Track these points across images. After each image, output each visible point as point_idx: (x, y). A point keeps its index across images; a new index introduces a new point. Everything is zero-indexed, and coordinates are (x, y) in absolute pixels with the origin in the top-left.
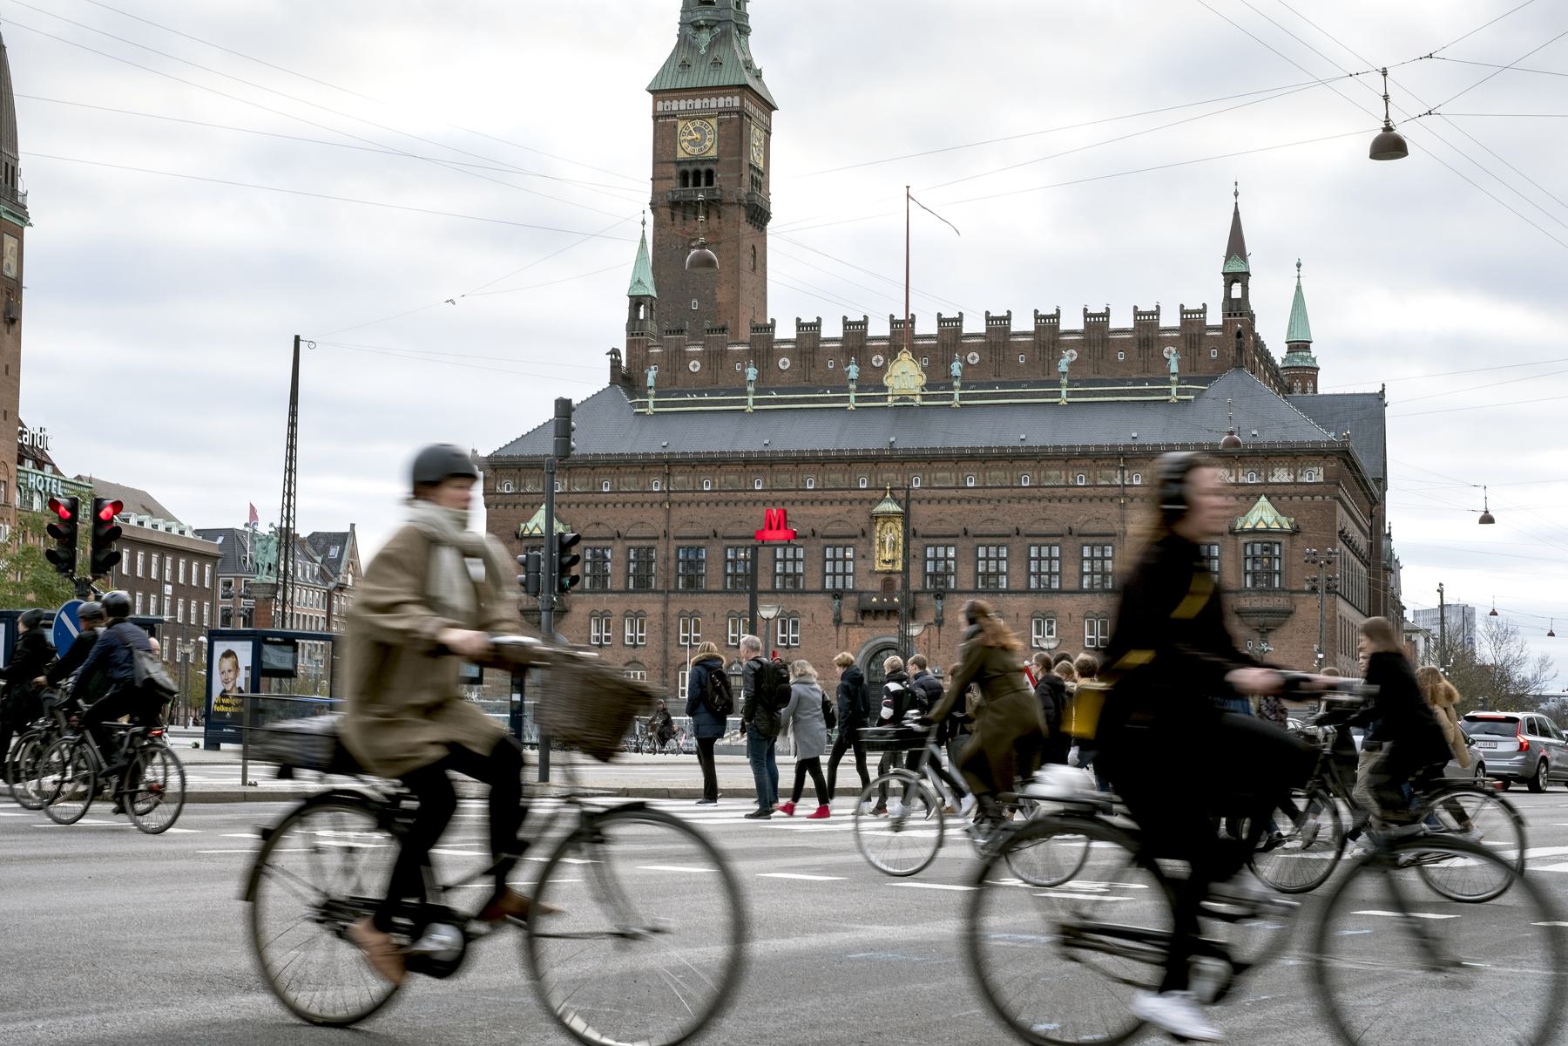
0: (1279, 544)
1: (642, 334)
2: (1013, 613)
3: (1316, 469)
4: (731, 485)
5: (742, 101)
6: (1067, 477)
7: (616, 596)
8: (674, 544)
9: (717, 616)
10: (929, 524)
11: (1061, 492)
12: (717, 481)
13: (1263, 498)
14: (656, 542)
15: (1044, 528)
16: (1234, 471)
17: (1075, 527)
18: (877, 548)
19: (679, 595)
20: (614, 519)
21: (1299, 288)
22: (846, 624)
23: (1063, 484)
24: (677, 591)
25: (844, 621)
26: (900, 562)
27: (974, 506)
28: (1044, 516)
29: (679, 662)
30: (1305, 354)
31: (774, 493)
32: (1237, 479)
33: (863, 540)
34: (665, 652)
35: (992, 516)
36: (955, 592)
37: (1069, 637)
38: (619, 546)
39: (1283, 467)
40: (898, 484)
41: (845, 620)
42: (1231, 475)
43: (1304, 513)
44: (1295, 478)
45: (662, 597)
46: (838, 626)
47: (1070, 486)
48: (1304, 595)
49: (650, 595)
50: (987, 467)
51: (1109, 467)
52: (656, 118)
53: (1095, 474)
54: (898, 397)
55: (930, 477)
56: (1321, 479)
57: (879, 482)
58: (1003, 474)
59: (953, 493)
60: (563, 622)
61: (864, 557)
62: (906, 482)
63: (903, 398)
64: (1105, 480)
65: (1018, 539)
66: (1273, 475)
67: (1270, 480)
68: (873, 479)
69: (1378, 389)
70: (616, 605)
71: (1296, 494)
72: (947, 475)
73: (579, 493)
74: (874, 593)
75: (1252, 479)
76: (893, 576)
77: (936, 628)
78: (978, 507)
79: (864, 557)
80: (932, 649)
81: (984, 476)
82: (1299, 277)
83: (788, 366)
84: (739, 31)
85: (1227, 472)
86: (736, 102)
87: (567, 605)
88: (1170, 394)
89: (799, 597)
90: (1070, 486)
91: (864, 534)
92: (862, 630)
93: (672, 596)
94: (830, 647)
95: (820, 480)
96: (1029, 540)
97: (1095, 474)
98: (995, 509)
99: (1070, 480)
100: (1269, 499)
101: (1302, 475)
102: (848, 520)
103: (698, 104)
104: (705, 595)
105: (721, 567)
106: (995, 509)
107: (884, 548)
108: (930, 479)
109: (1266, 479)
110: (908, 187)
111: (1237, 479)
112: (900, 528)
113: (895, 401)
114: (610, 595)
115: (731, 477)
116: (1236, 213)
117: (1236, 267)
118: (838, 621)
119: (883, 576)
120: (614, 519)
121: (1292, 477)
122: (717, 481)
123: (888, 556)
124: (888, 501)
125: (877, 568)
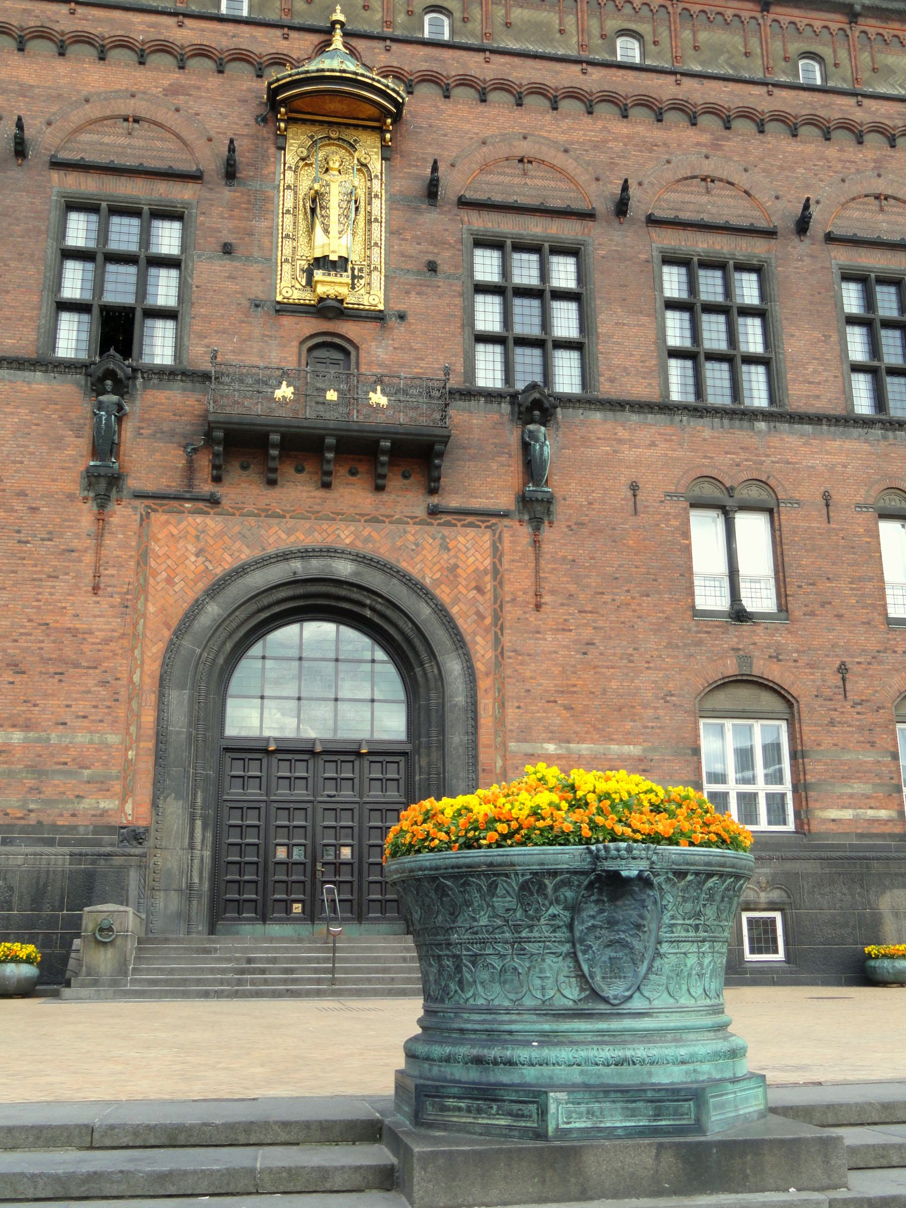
2: (810, 492)
10: (484, 168)
22: (139, 496)
25: (133, 483)
26: (378, 279)
28: (881, 186)
33: (227, 194)
35: (708, 168)
46: (102, 502)
55: (487, 18)
58: (738, 40)
59: (569, 76)
62: (401, 18)
65: (800, 248)
76: (349, 329)
77: (525, 531)
78: (657, 134)
79: (227, 250)
80: (511, 613)
81: (674, 35)
91: (230, 173)
92: (212, 523)
96: (843, 257)
98: (717, 147)
102: (162, 115)
106: (717, 147)
112: (376, 165)
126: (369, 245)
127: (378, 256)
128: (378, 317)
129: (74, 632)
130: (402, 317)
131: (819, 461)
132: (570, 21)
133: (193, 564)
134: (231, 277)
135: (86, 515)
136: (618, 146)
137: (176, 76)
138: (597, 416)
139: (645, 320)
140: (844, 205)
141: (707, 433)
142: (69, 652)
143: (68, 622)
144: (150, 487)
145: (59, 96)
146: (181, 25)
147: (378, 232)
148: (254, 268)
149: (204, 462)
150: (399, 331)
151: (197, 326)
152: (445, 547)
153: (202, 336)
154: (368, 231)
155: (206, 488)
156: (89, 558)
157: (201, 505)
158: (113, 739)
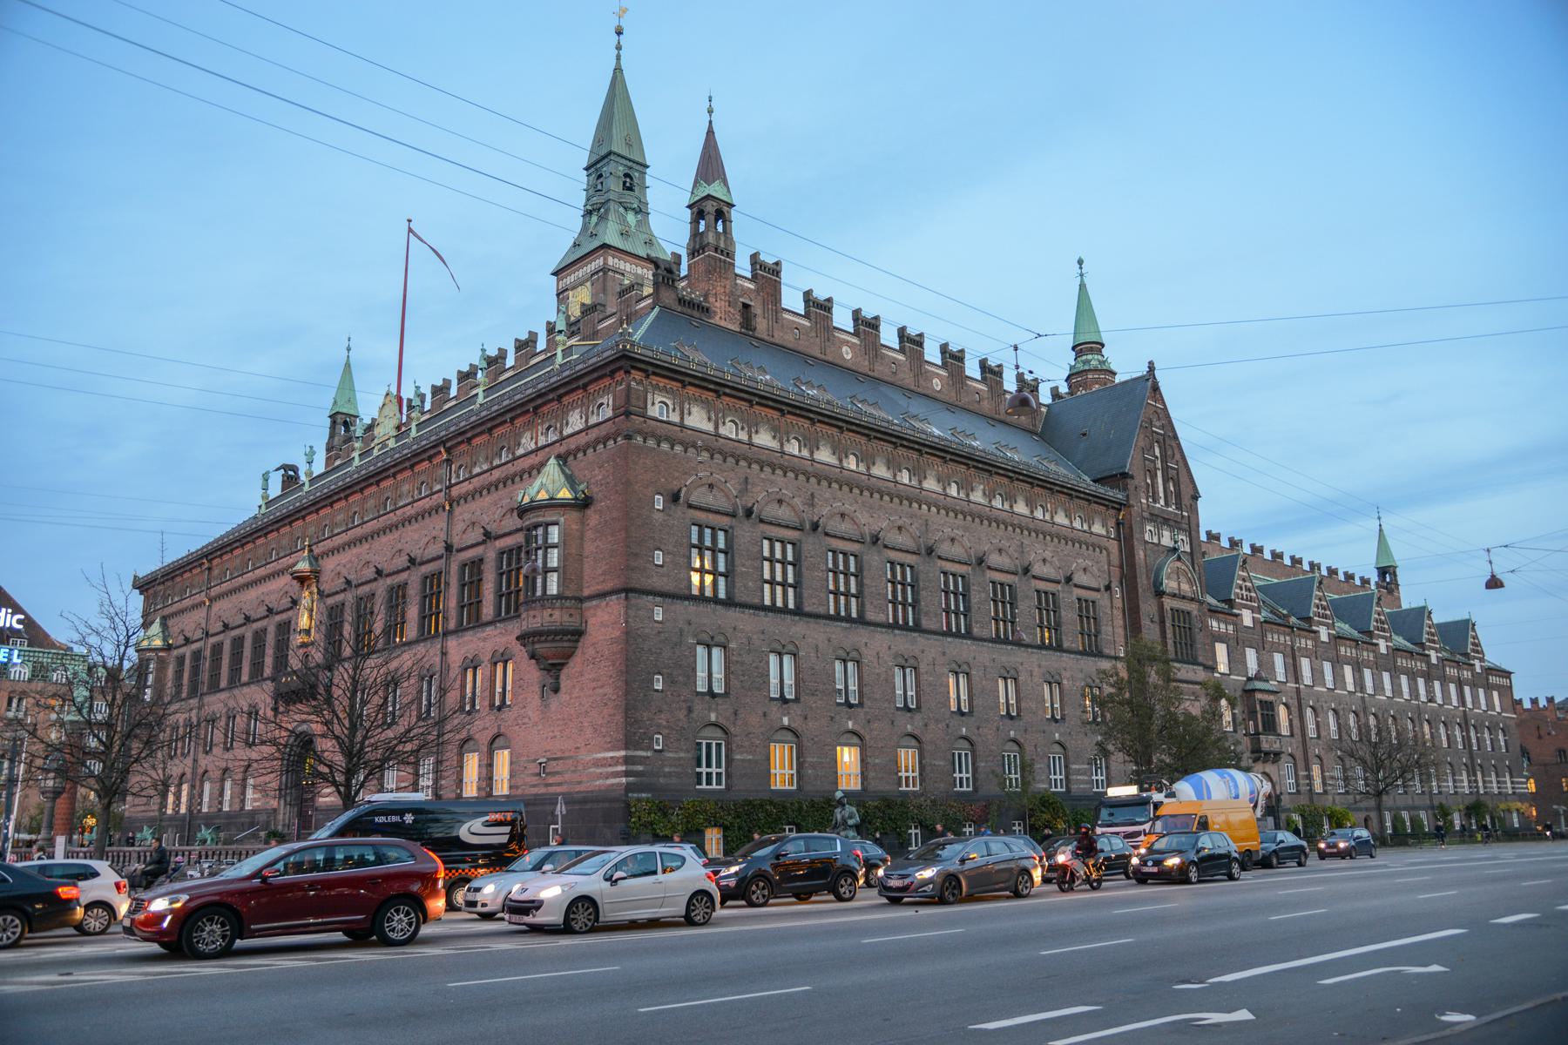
3: (604, 400)
5: (605, 259)
11: (409, 511)
13: (552, 461)
21: (1082, 287)
30: (1090, 357)
32: (536, 443)
38: (187, 651)
39: (576, 408)
44: (587, 421)
48: (594, 603)
51: (439, 465)
52: (558, 295)
56: (609, 413)
63: (384, 444)
66: (567, 424)
67: (565, 433)
69: (1143, 370)
71: (588, 446)
82: (1082, 275)
84: (626, 209)
86: (600, 262)
99: (416, 492)
103: (580, 273)
109: (561, 432)
110: (409, 221)
111: (536, 443)
116: (710, 132)
117: (705, 190)
119: (301, 651)
128: (312, 643)
140: (392, 559)
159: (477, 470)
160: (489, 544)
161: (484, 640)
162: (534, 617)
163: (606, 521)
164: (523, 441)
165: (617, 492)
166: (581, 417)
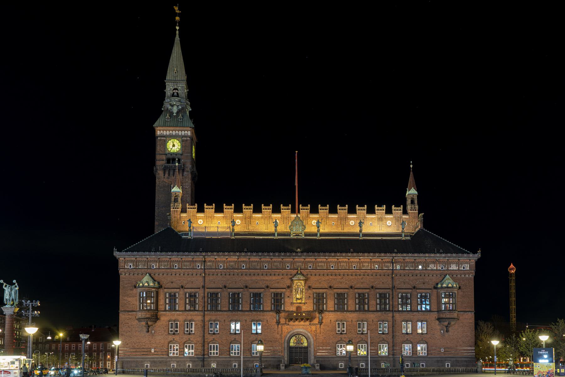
0: (455, 293)
1: (178, 208)
2: (350, 320)
4: (231, 267)
6: (371, 266)
7: (180, 312)
8: (207, 290)
9: (226, 321)
12: (225, 265)
14: (198, 290)
15: (362, 286)
16: (436, 265)
17: (374, 285)
18: (294, 293)
19: (209, 312)
20: (180, 280)
23: (370, 269)
24: (208, 311)
26: (304, 299)
27: (334, 277)
29: (209, 341)
31: (250, 270)
32: (437, 268)
34: (204, 336)
36: (326, 311)
37: (372, 329)
38: (182, 291)
40: (303, 267)
41: (282, 323)
42: (435, 266)
43: (462, 281)
44: (459, 268)
45: (202, 313)
46: (278, 325)
47: (372, 270)
48: (462, 313)
49: (196, 312)
50: (339, 262)
53: (382, 265)
54: (295, 235)
55: (316, 265)
57: (295, 266)
58: (346, 264)
60: (156, 324)
61: (288, 297)
64: (386, 267)
65: (351, 290)
66: (450, 267)
67: (449, 269)
68: (292, 265)
70: (180, 317)
72: (323, 264)
73: (163, 269)
74: (295, 312)
75: (442, 268)
76: (301, 305)
77: (319, 326)
79: (288, 297)
80: (318, 334)
83: (240, 223)
85: (433, 265)
87: (159, 317)
88: (402, 236)
89: (261, 313)
90: (372, 270)
92: (288, 327)
93: (206, 312)
94: (275, 333)
95: (270, 265)
97: (382, 265)
98: (342, 278)
99: (372, 267)
100: (449, 275)
101: (461, 267)
104: (221, 312)
105: (227, 301)
107: (297, 292)
108: (316, 265)
109: (448, 268)
111: (437, 268)
113: (294, 236)
114: (178, 312)
115: (232, 264)
118: (278, 323)
120: (180, 280)
121: (457, 268)
122: (225, 265)
123: (298, 296)
124: (299, 274)
125: (295, 302)
126: (303, 294)
127: (304, 297)
128: (304, 303)
129: (276, 338)
130: (306, 303)
131: (351, 316)
132: (325, 264)
133: (286, 331)
134: (289, 300)
135: (276, 326)
136: (330, 280)
137: (282, 277)
138: (327, 313)
139: (332, 301)
141: (339, 314)
142: (276, 340)
143: (275, 337)
144: (282, 323)
145: (271, 281)
146: (282, 271)
147: (304, 293)
148: (291, 299)
149: (287, 320)
150: (306, 304)
151: (286, 306)
152: (311, 328)
153: (286, 307)
154: (303, 293)
155: (288, 323)
156: (277, 331)
157: (287, 325)
158: (280, 348)
159: (407, 268)
160: (414, 290)
161: (413, 316)
162: (452, 315)
163: (466, 295)
164: (430, 266)
165: (470, 288)
166: (456, 267)
